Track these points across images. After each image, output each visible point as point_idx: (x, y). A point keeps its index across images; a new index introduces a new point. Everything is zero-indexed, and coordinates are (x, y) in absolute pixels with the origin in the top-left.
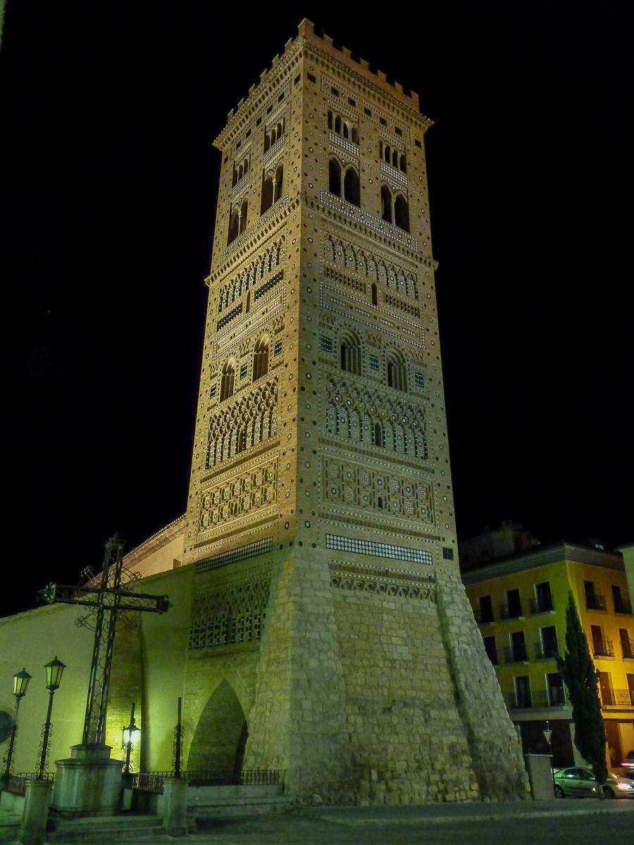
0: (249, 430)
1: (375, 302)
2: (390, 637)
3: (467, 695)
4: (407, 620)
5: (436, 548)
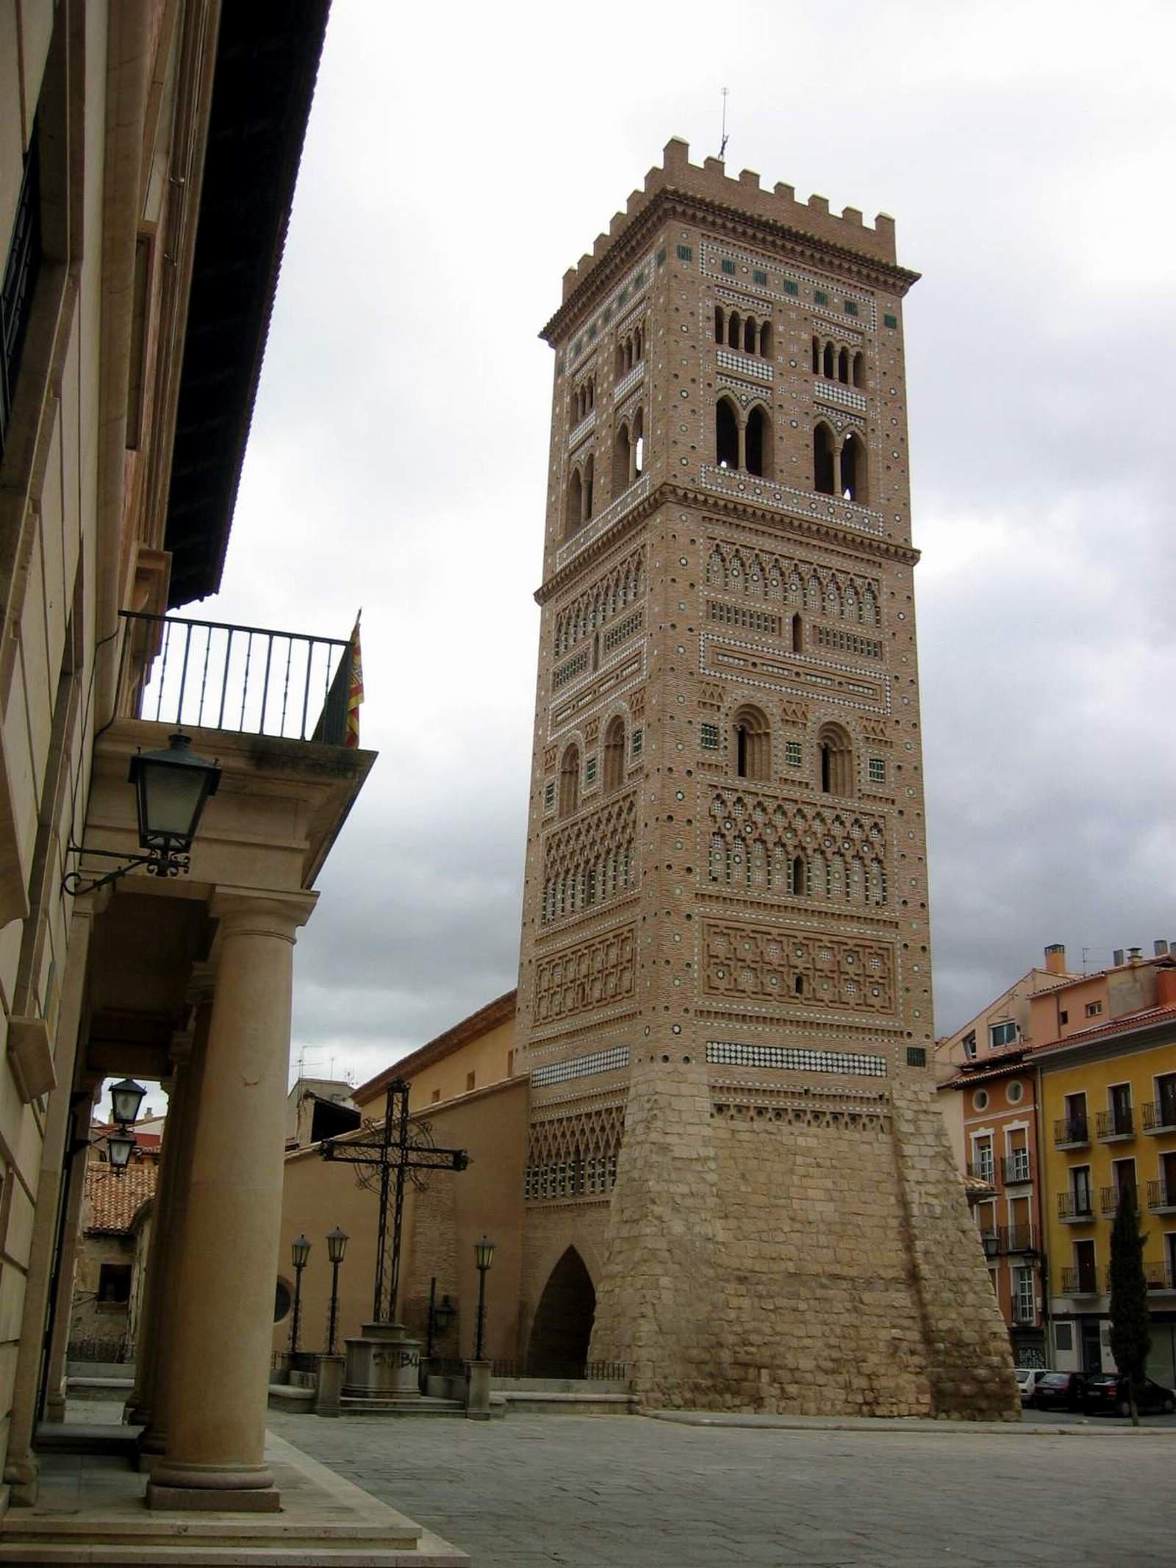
0: (600, 868)
1: (797, 647)
2: (805, 1188)
3: (925, 1270)
5: (898, 1051)
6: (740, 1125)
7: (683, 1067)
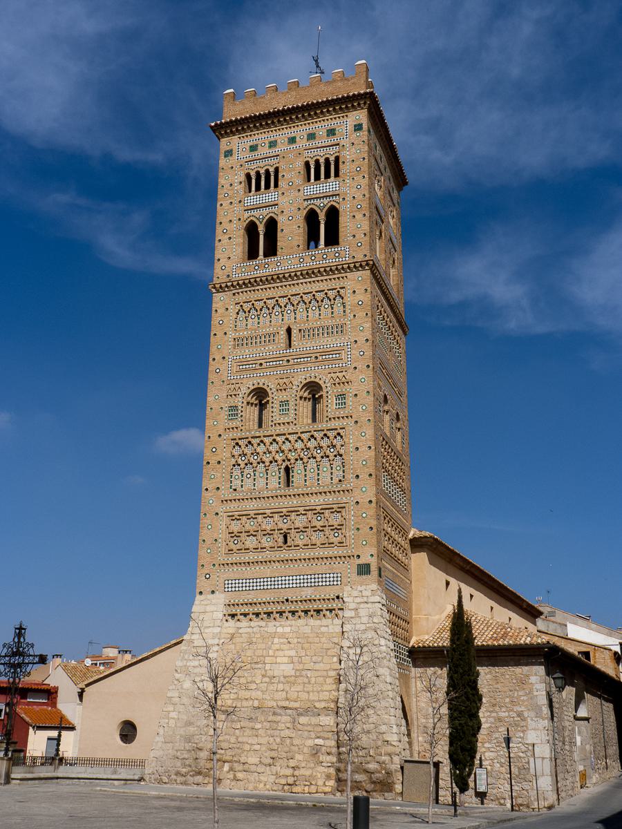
2: (276, 657)
4: (299, 640)
5: (350, 568)
6: (244, 623)
7: (210, 596)
